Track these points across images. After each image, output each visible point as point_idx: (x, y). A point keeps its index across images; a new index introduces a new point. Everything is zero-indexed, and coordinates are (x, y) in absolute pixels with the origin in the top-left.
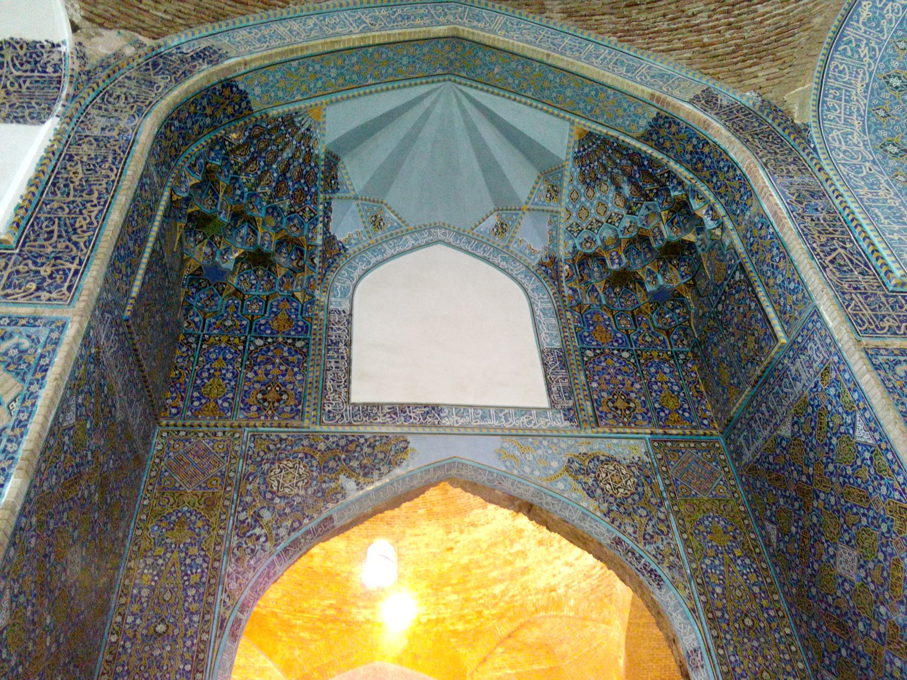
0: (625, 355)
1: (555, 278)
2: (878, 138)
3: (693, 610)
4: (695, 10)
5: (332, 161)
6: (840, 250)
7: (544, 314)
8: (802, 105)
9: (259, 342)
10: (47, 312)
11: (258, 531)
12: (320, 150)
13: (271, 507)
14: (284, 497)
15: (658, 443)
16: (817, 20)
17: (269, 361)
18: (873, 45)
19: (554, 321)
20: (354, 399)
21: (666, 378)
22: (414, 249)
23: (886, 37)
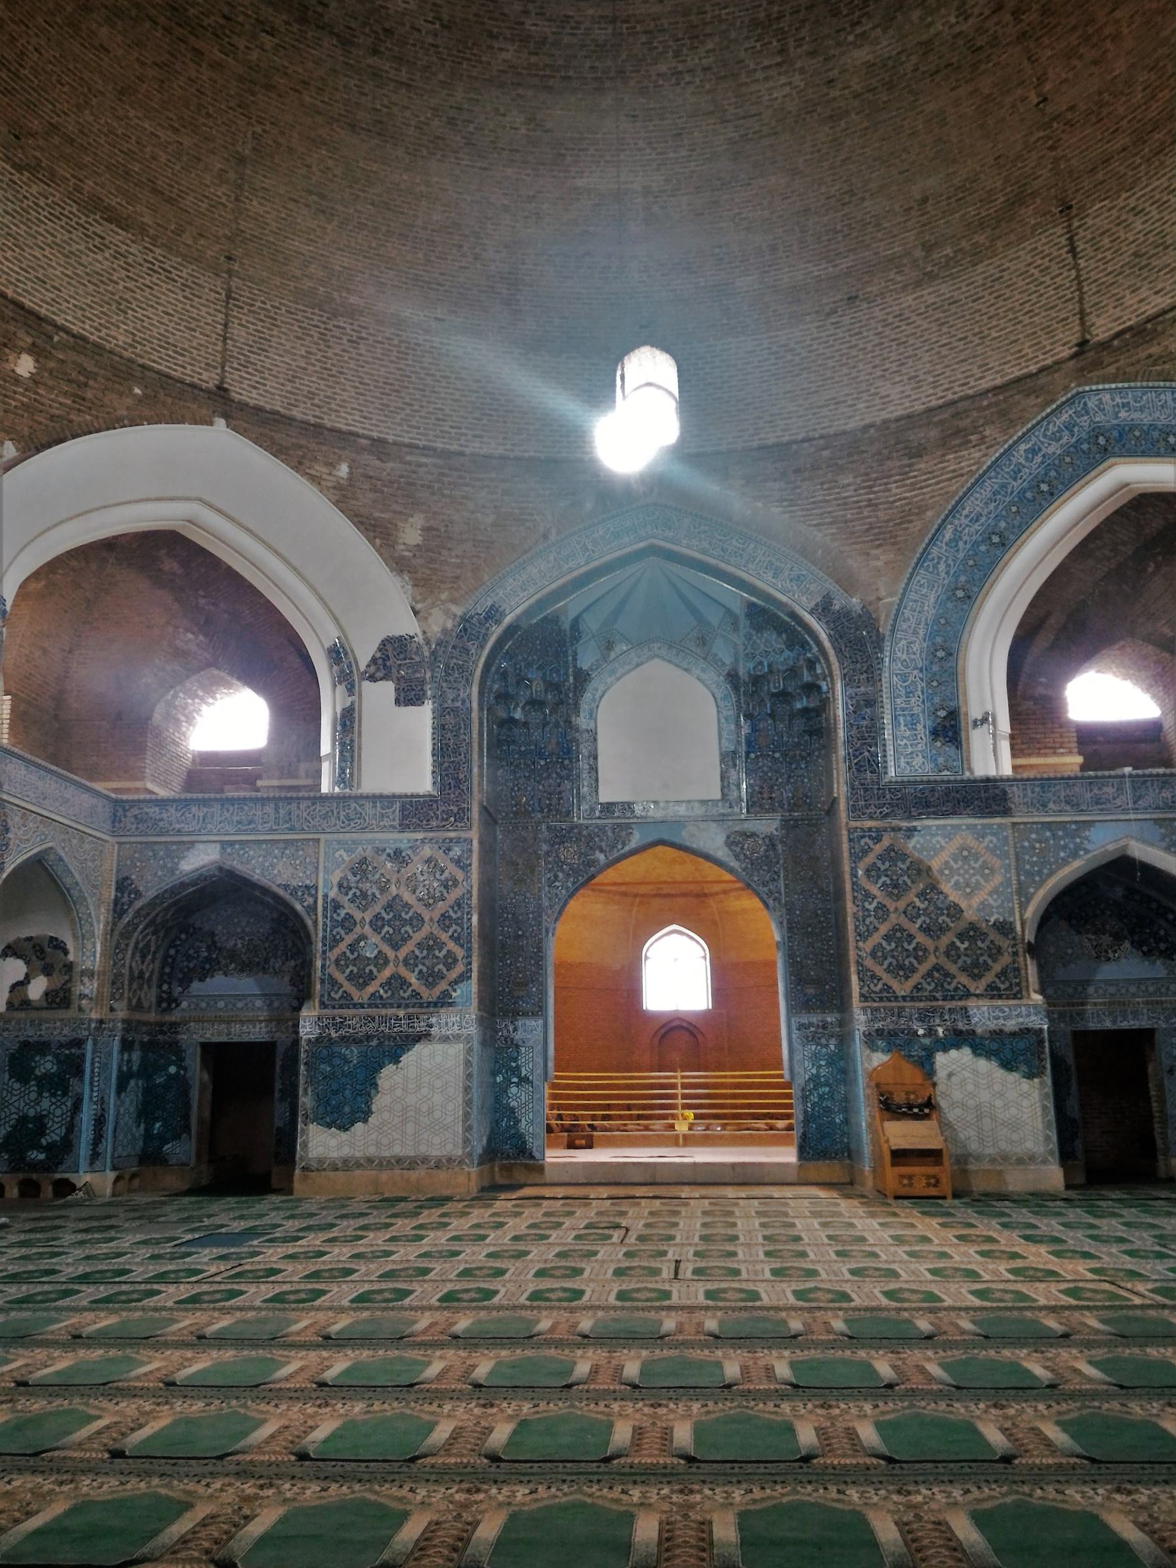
0: (777, 755)
1: (736, 688)
2: (934, 644)
3: (781, 923)
4: (846, 482)
5: (575, 624)
6: (866, 754)
7: (726, 720)
8: (887, 616)
9: (542, 763)
10: (463, 835)
11: (557, 884)
12: (566, 626)
13: (563, 871)
14: (569, 864)
15: (786, 824)
16: (929, 514)
17: (549, 777)
18: (950, 562)
19: (733, 727)
20: (601, 801)
21: (800, 772)
22: (637, 666)
23: (961, 555)
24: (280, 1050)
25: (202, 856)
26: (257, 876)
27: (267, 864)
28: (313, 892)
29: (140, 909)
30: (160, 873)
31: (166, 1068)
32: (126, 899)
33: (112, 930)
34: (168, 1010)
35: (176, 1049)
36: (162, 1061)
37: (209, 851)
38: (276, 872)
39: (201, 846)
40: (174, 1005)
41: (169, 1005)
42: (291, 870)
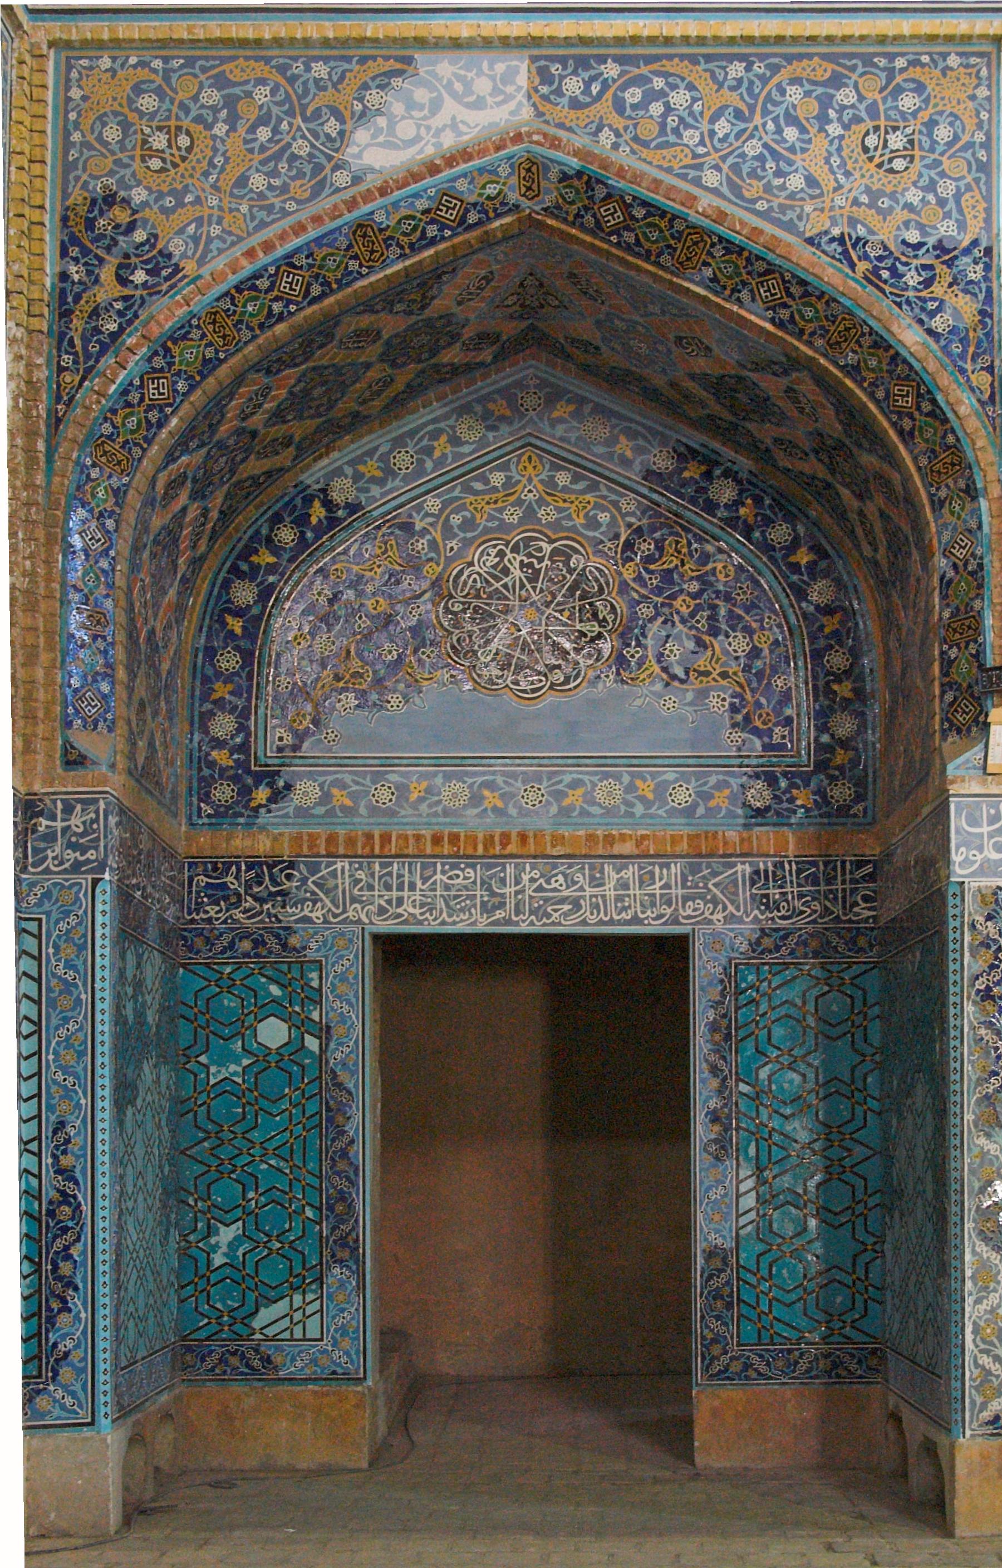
24: (705, 969)
25: (450, 108)
26: (708, 197)
27: (753, 148)
28: (975, 273)
29: (180, 335)
30: (258, 182)
31: (243, 1028)
32: (107, 289)
33: (56, 422)
34: (241, 810)
35: (277, 951)
36: (229, 1002)
37: (483, 86)
38: (796, 182)
39: (445, 67)
40: (262, 794)
41: (246, 792)
42: (868, 175)
